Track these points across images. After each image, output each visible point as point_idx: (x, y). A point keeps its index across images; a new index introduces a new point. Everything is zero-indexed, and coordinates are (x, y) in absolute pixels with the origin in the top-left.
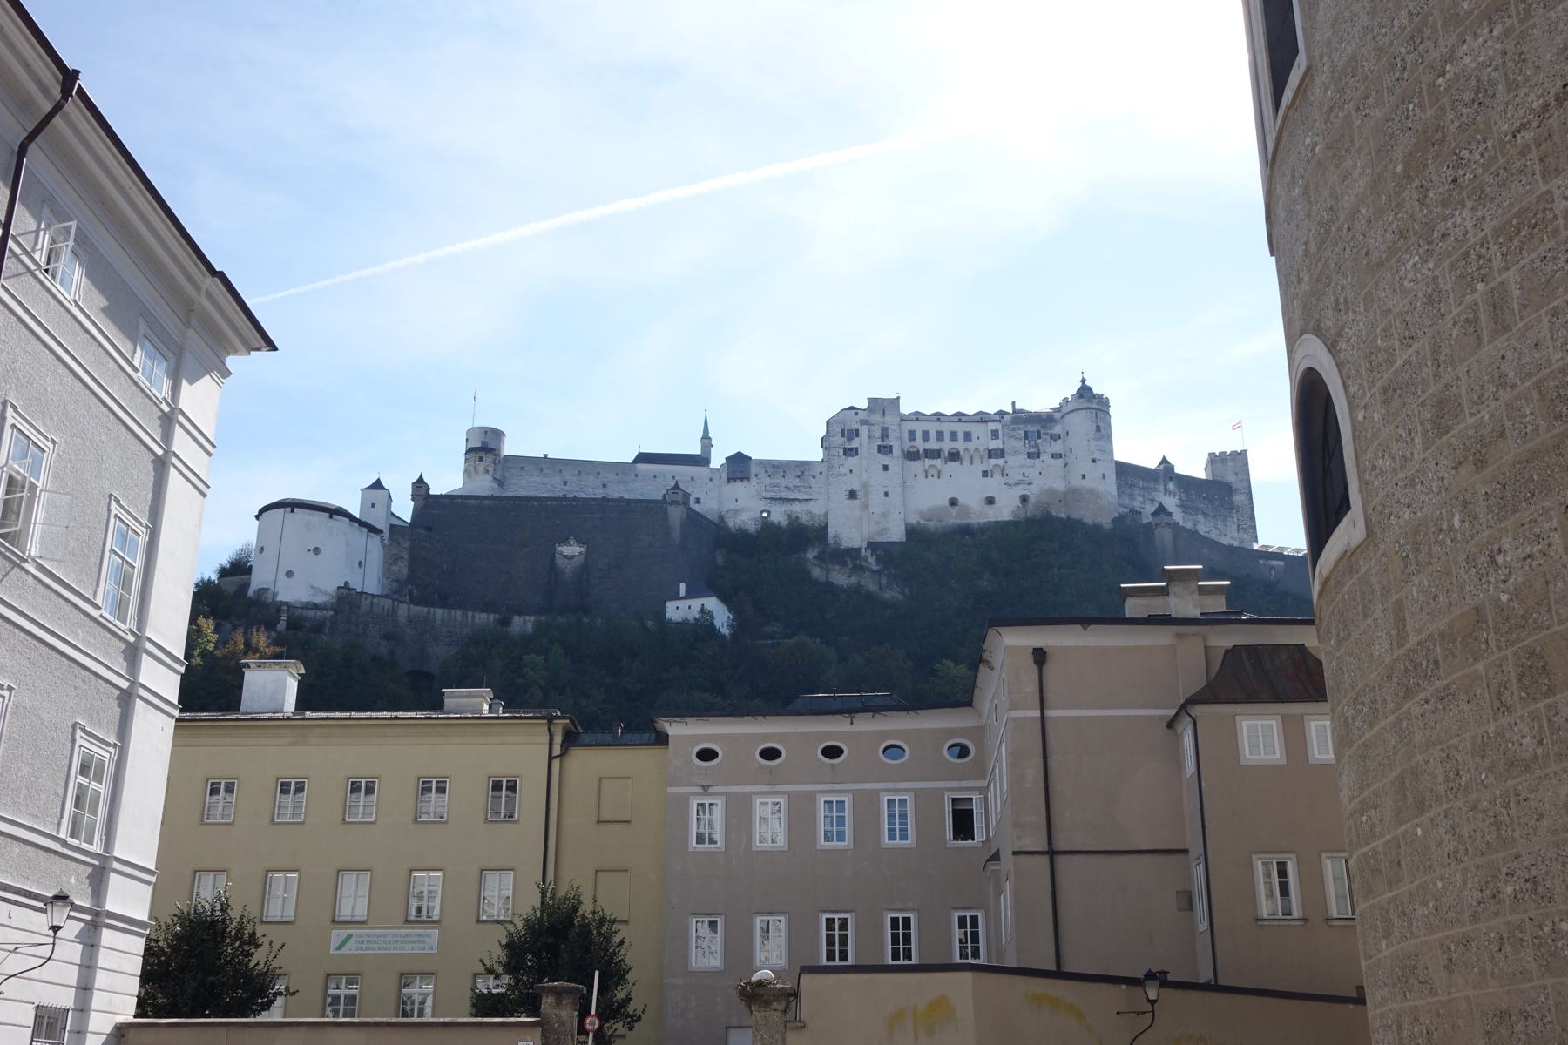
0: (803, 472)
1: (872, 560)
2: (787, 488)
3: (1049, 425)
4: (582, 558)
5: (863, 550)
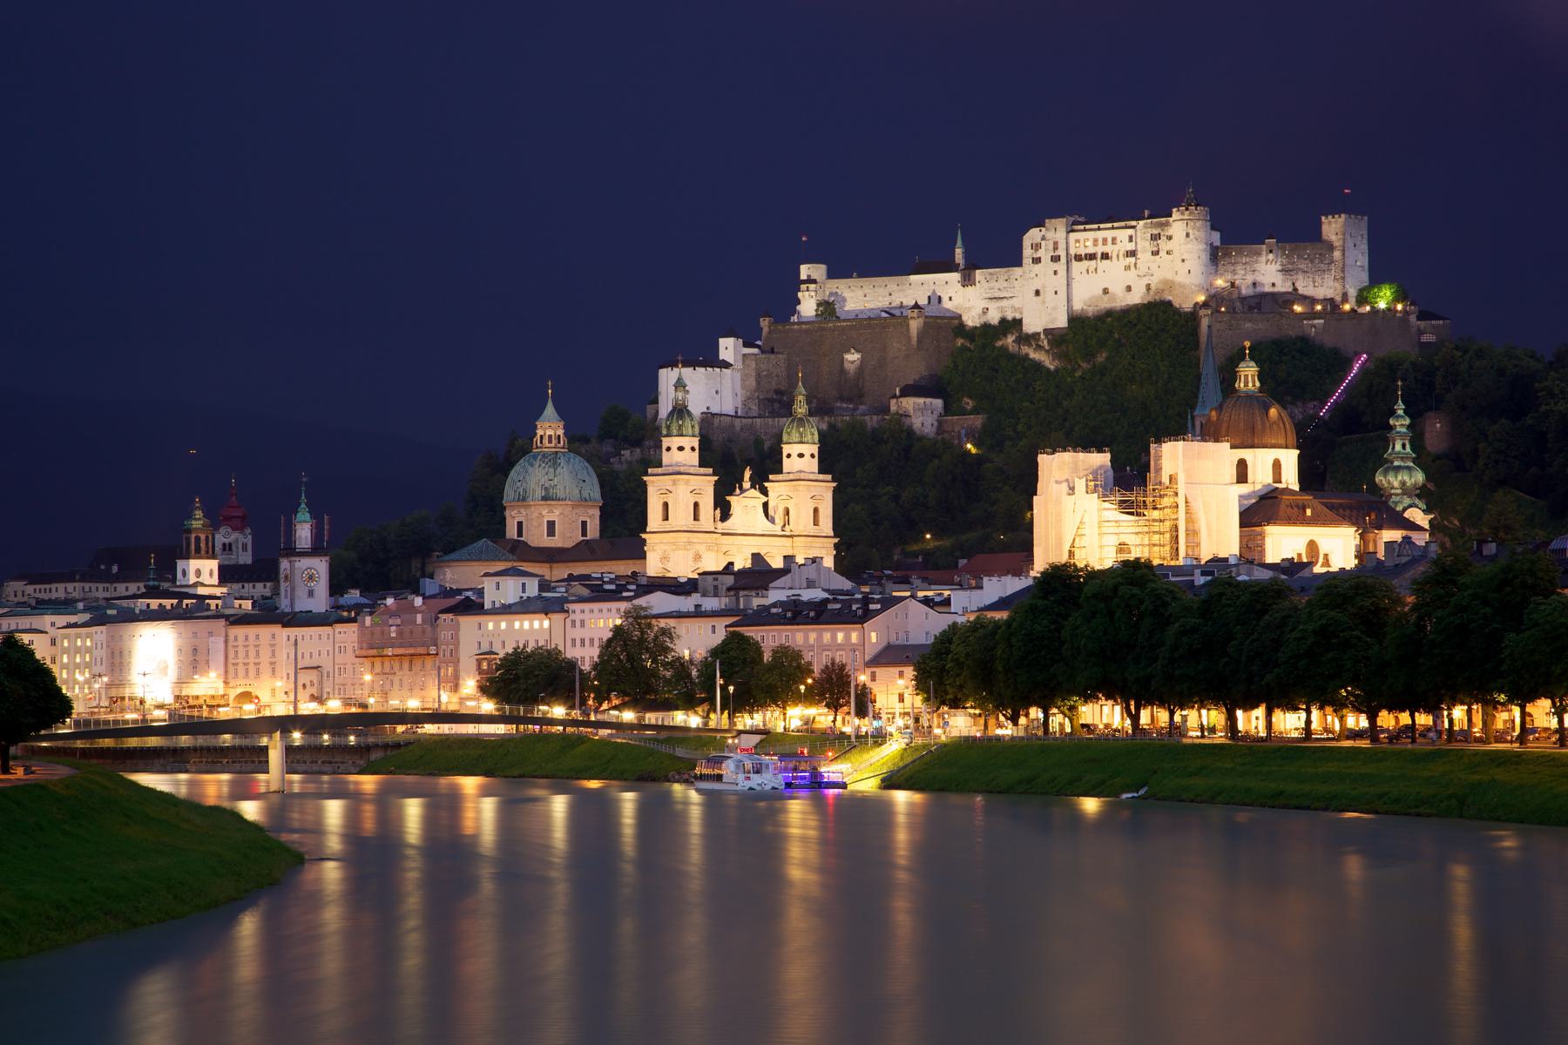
0: (1009, 276)
1: (1046, 342)
2: (999, 289)
3: (1166, 228)
4: (859, 362)
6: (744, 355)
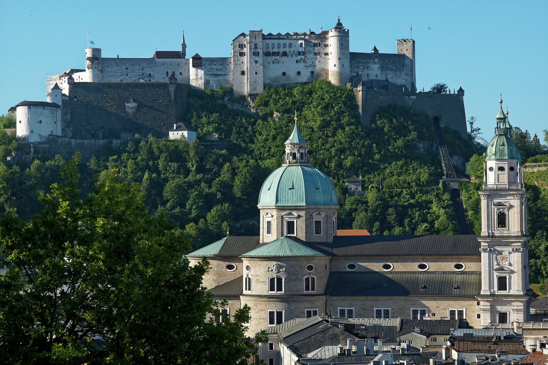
2: (217, 70)
4: (136, 108)
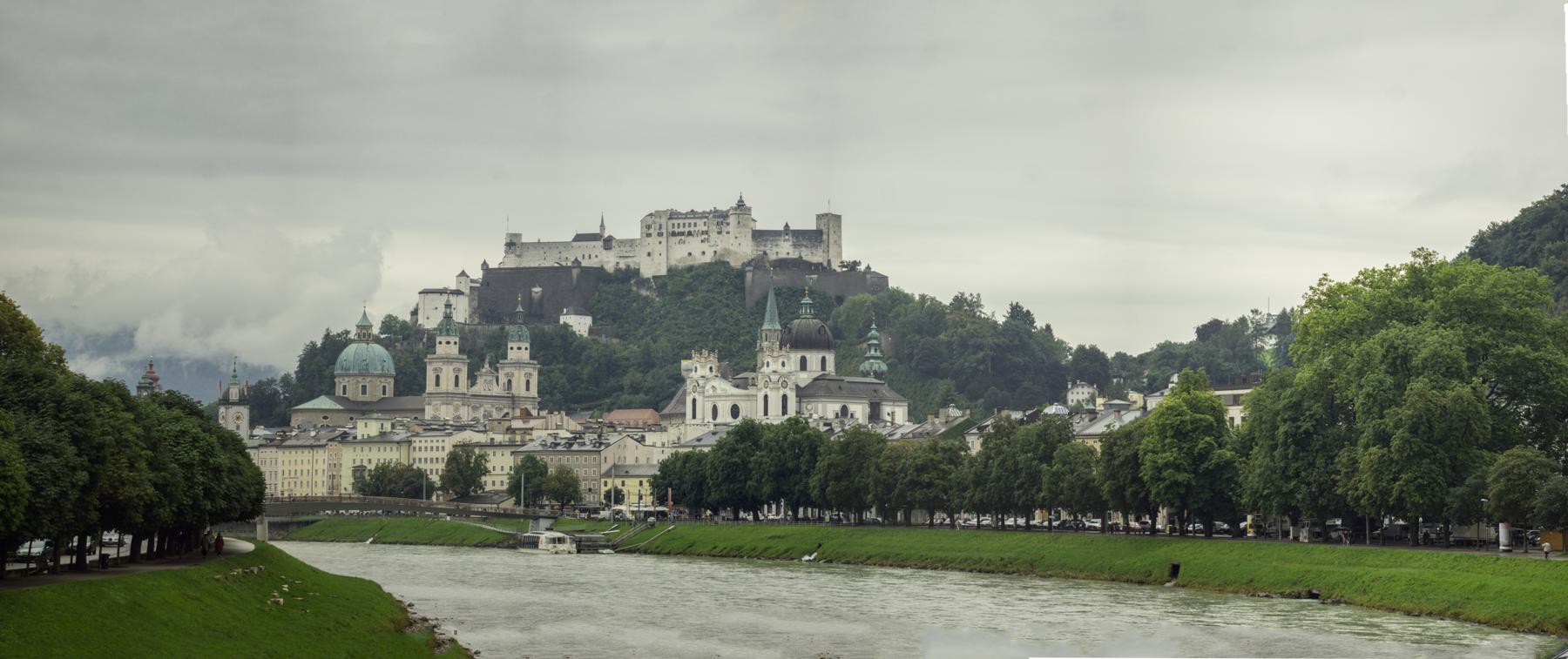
5: (652, 280)
6: (471, 287)
